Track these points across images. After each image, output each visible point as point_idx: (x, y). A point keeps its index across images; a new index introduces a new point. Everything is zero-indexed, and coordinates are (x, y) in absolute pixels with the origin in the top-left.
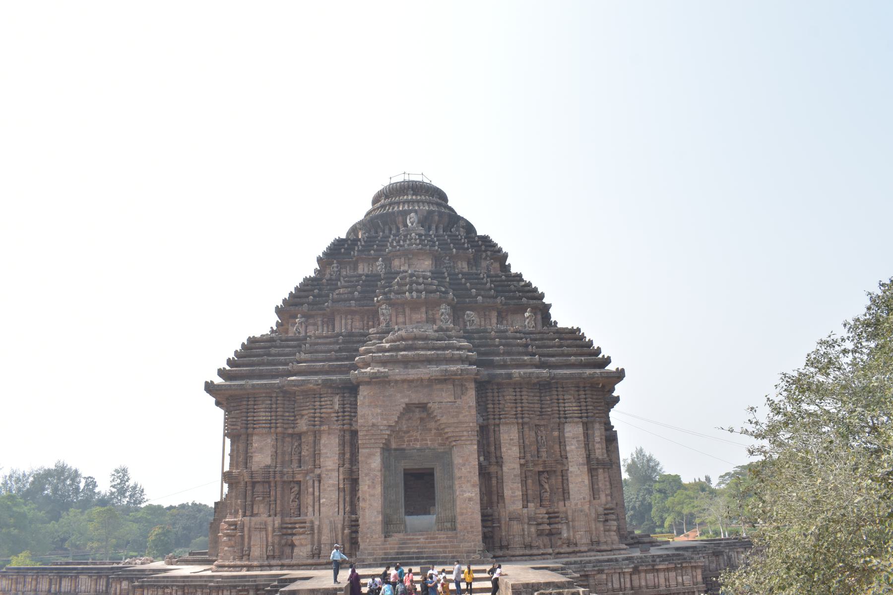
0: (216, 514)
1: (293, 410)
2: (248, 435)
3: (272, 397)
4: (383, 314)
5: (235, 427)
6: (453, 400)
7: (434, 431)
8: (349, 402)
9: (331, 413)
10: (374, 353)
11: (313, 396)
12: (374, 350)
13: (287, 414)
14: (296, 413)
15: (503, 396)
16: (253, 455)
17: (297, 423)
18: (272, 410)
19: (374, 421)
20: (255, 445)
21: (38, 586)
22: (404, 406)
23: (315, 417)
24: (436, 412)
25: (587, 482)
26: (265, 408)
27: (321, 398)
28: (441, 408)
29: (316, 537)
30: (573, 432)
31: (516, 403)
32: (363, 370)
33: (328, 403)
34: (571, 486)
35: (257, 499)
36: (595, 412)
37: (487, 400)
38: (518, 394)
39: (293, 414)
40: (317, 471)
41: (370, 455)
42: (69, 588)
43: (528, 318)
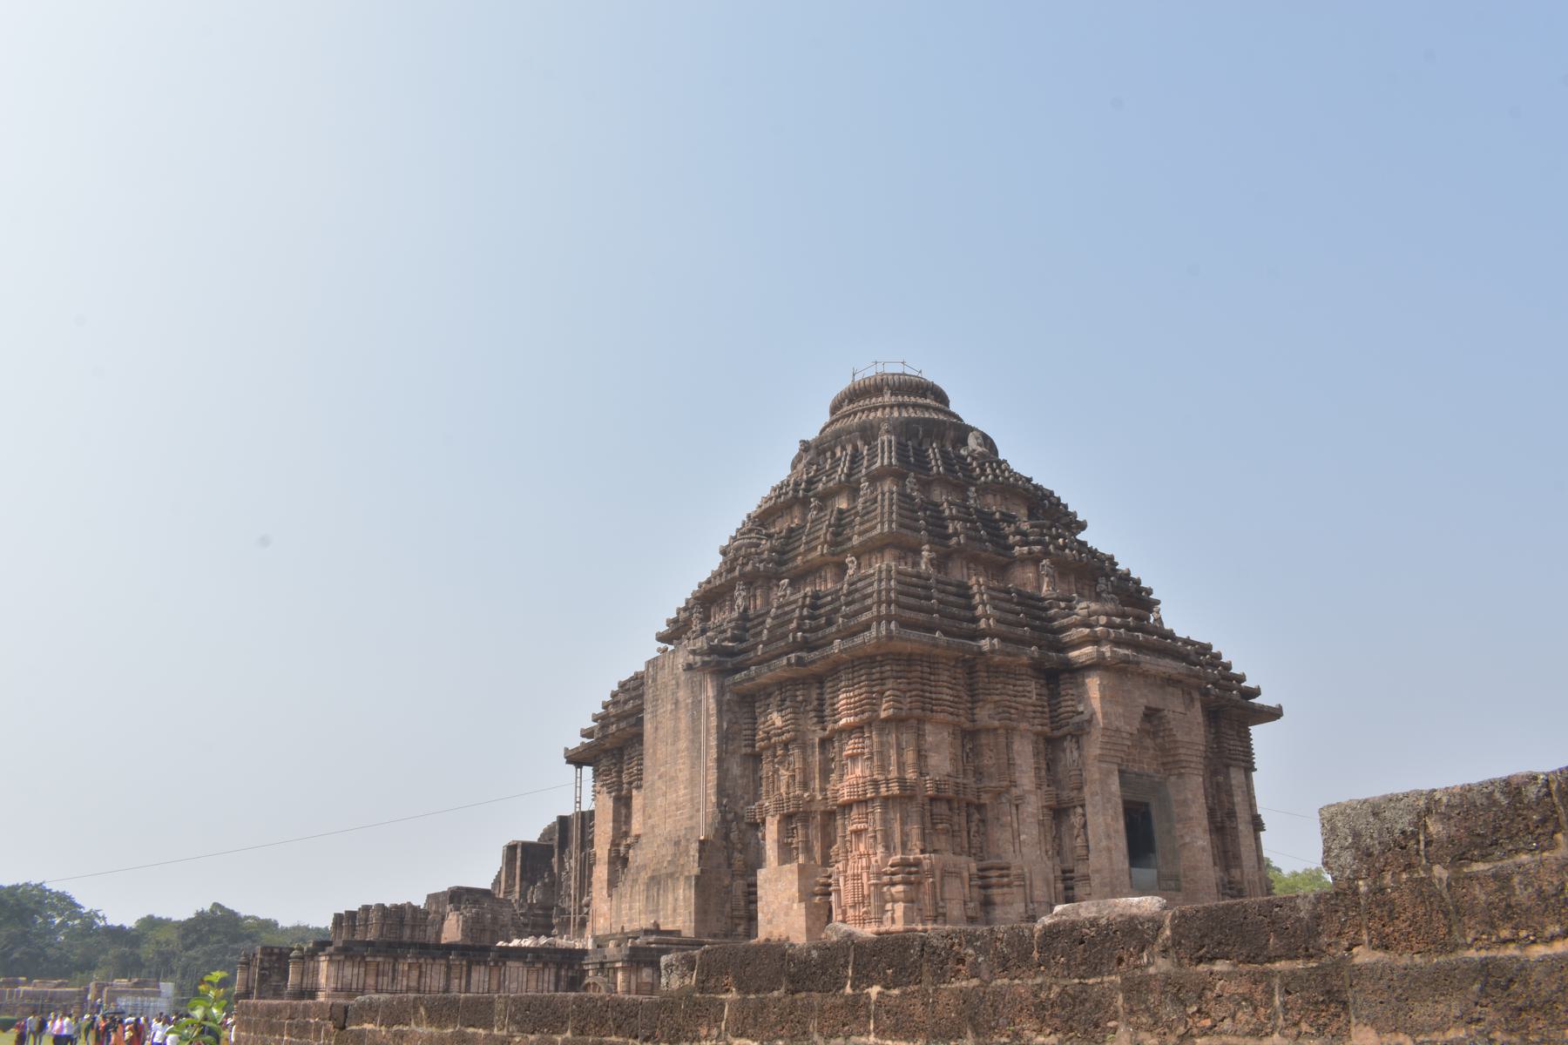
0: (702, 861)
7: (1151, 752)
14: (981, 697)
16: (926, 754)
19: (1117, 723)
20: (929, 739)
21: (423, 980)
22: (1143, 708)
25: (1254, 846)
29: (1028, 891)
30: (1236, 776)
34: (1242, 849)
35: (940, 826)
39: (969, 699)
40: (1015, 791)
41: (1108, 773)
42: (487, 987)
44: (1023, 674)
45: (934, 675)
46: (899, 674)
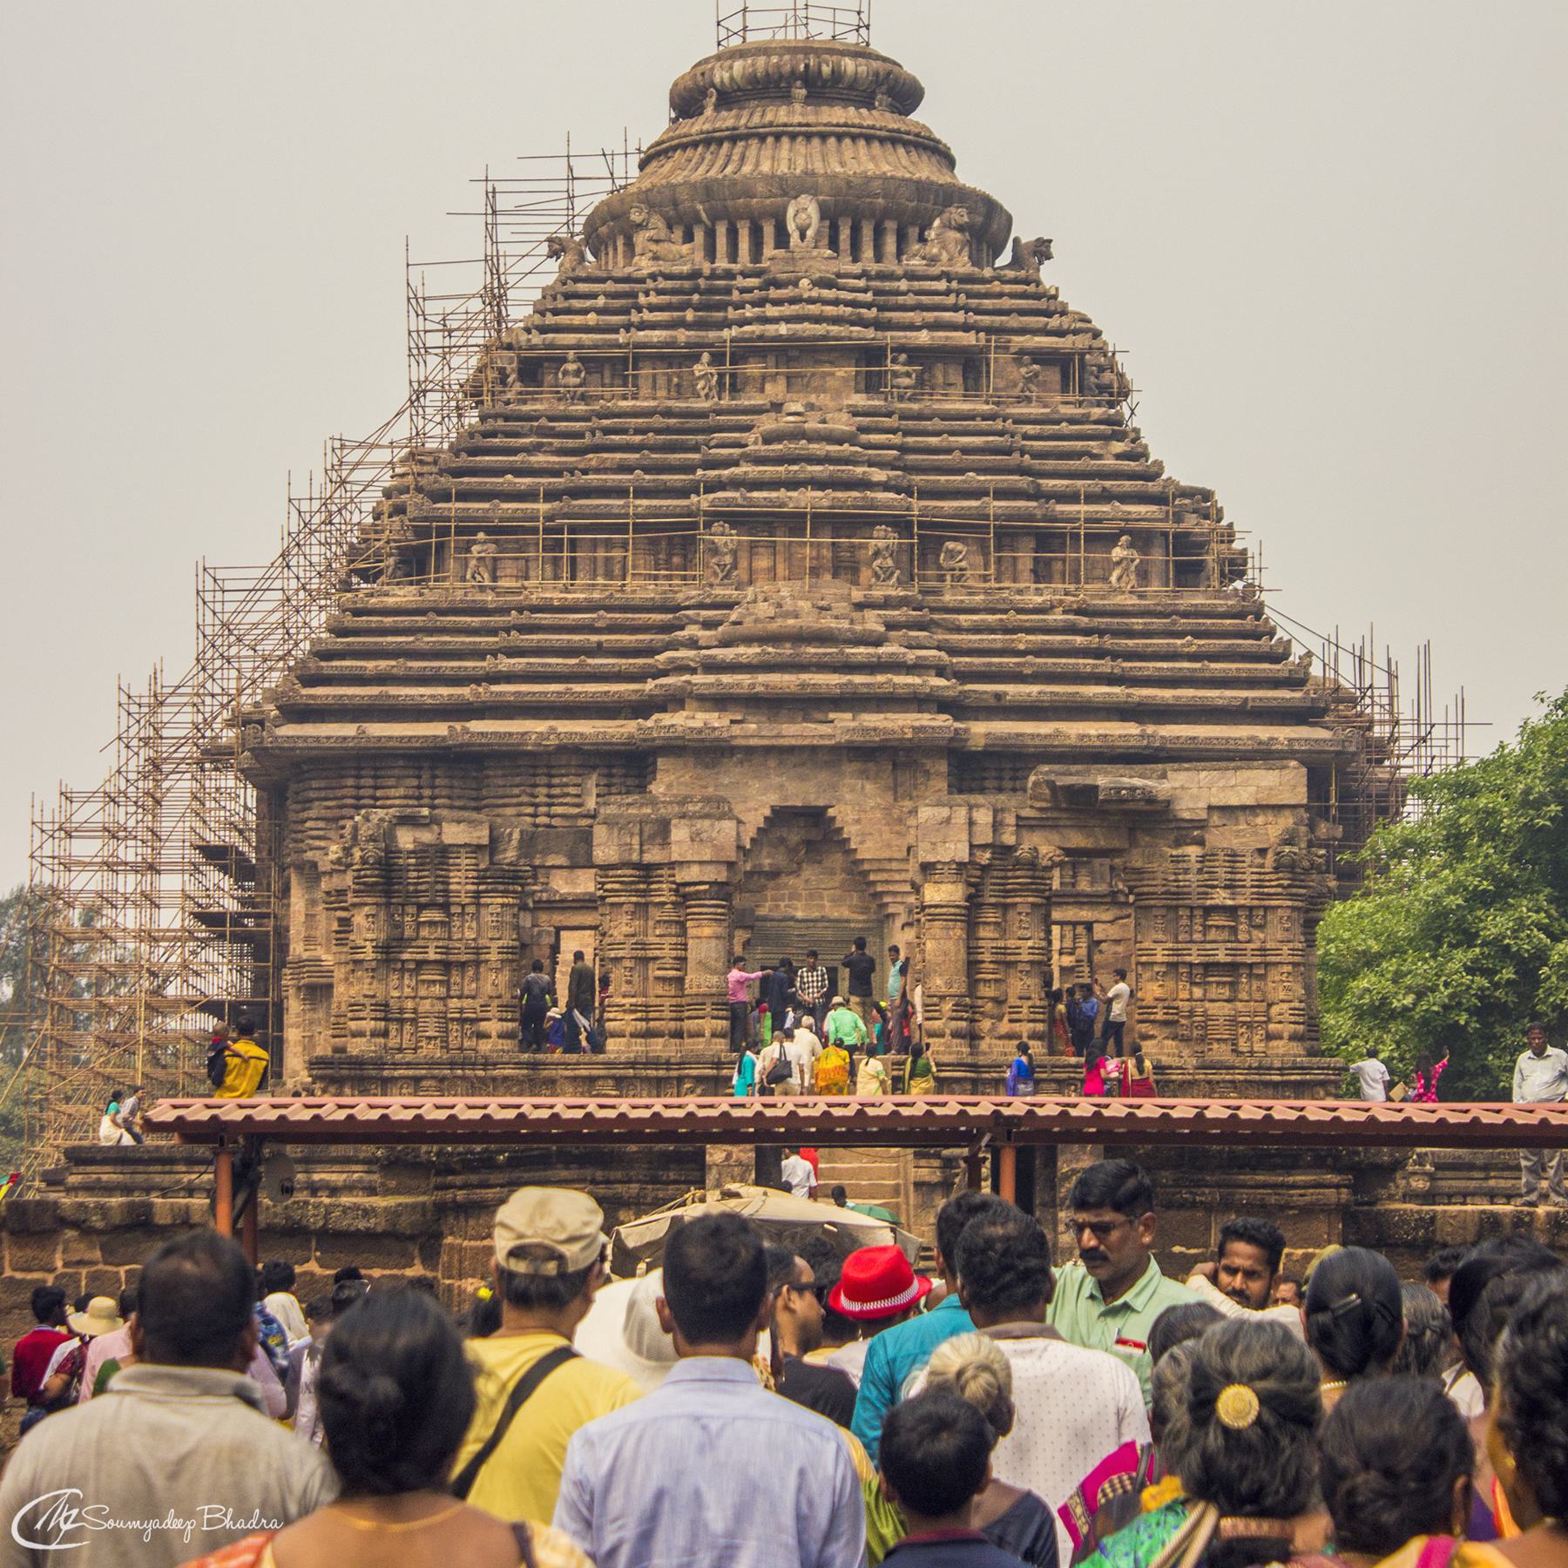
7: (840, 877)
9: (576, 817)
10: (693, 671)
22: (767, 812)
26: (405, 797)
27: (551, 776)
28: (858, 821)
33: (572, 790)
43: (1119, 563)
46: (323, 794)
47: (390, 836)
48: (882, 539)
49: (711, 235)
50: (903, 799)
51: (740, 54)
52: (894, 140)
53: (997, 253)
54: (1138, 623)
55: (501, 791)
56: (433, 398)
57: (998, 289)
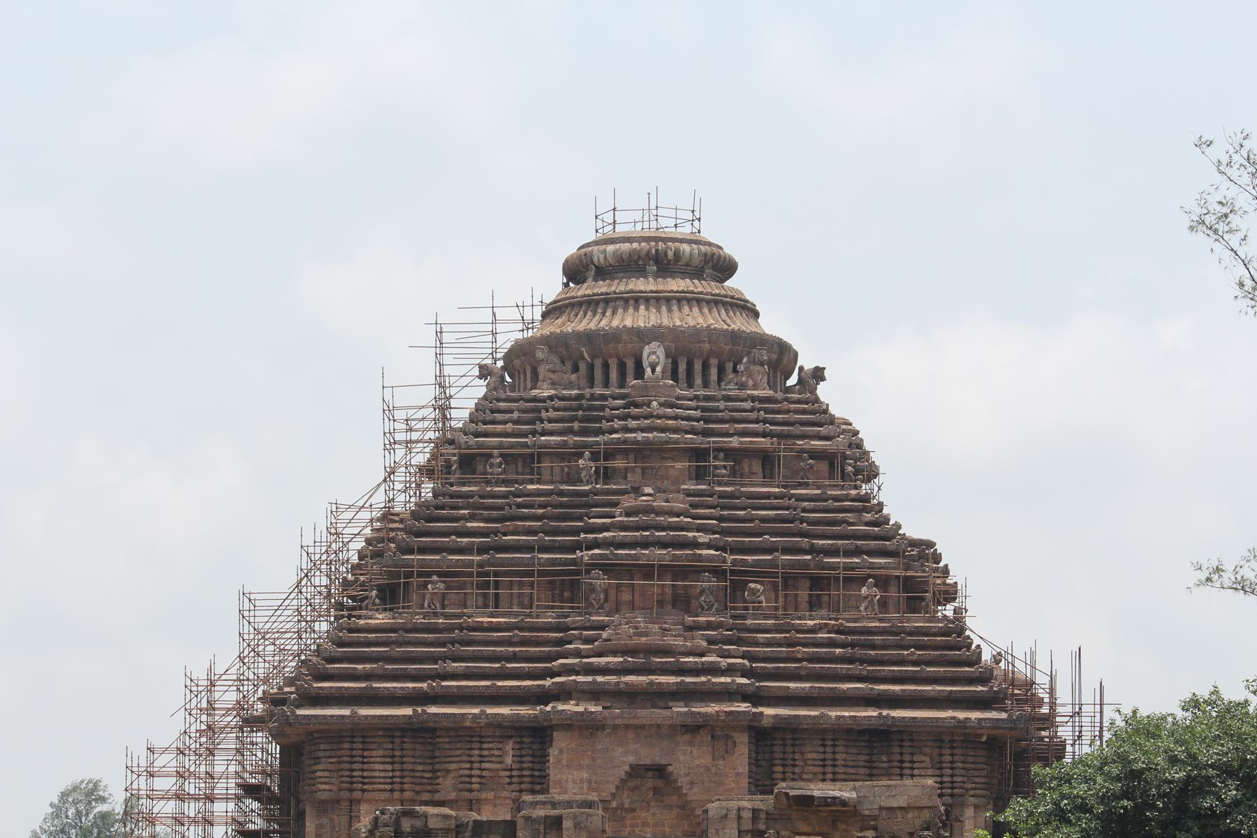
1: (429, 761)
2: (351, 801)
3: (393, 737)
4: (593, 590)
5: (327, 787)
6: (707, 760)
7: (676, 811)
8: (530, 752)
10: (578, 673)
11: (468, 739)
12: (576, 668)
13: (420, 768)
15: (802, 753)
17: (438, 784)
18: (395, 759)
22: (627, 768)
23: (471, 776)
24: (680, 780)
26: (384, 756)
27: (482, 742)
28: (688, 775)
31: (824, 766)
32: (561, 707)
33: (496, 753)
36: (969, 786)
37: (774, 759)
38: (829, 749)
39: (430, 768)
43: (866, 598)
44: (489, 736)
45: (368, 750)
46: (328, 753)
47: (397, 823)
48: (708, 583)
49: (591, 367)
50: (719, 760)
51: (612, 241)
52: (716, 302)
53: (788, 377)
54: (878, 638)
55: (448, 753)
56: (400, 476)
57: (786, 408)
